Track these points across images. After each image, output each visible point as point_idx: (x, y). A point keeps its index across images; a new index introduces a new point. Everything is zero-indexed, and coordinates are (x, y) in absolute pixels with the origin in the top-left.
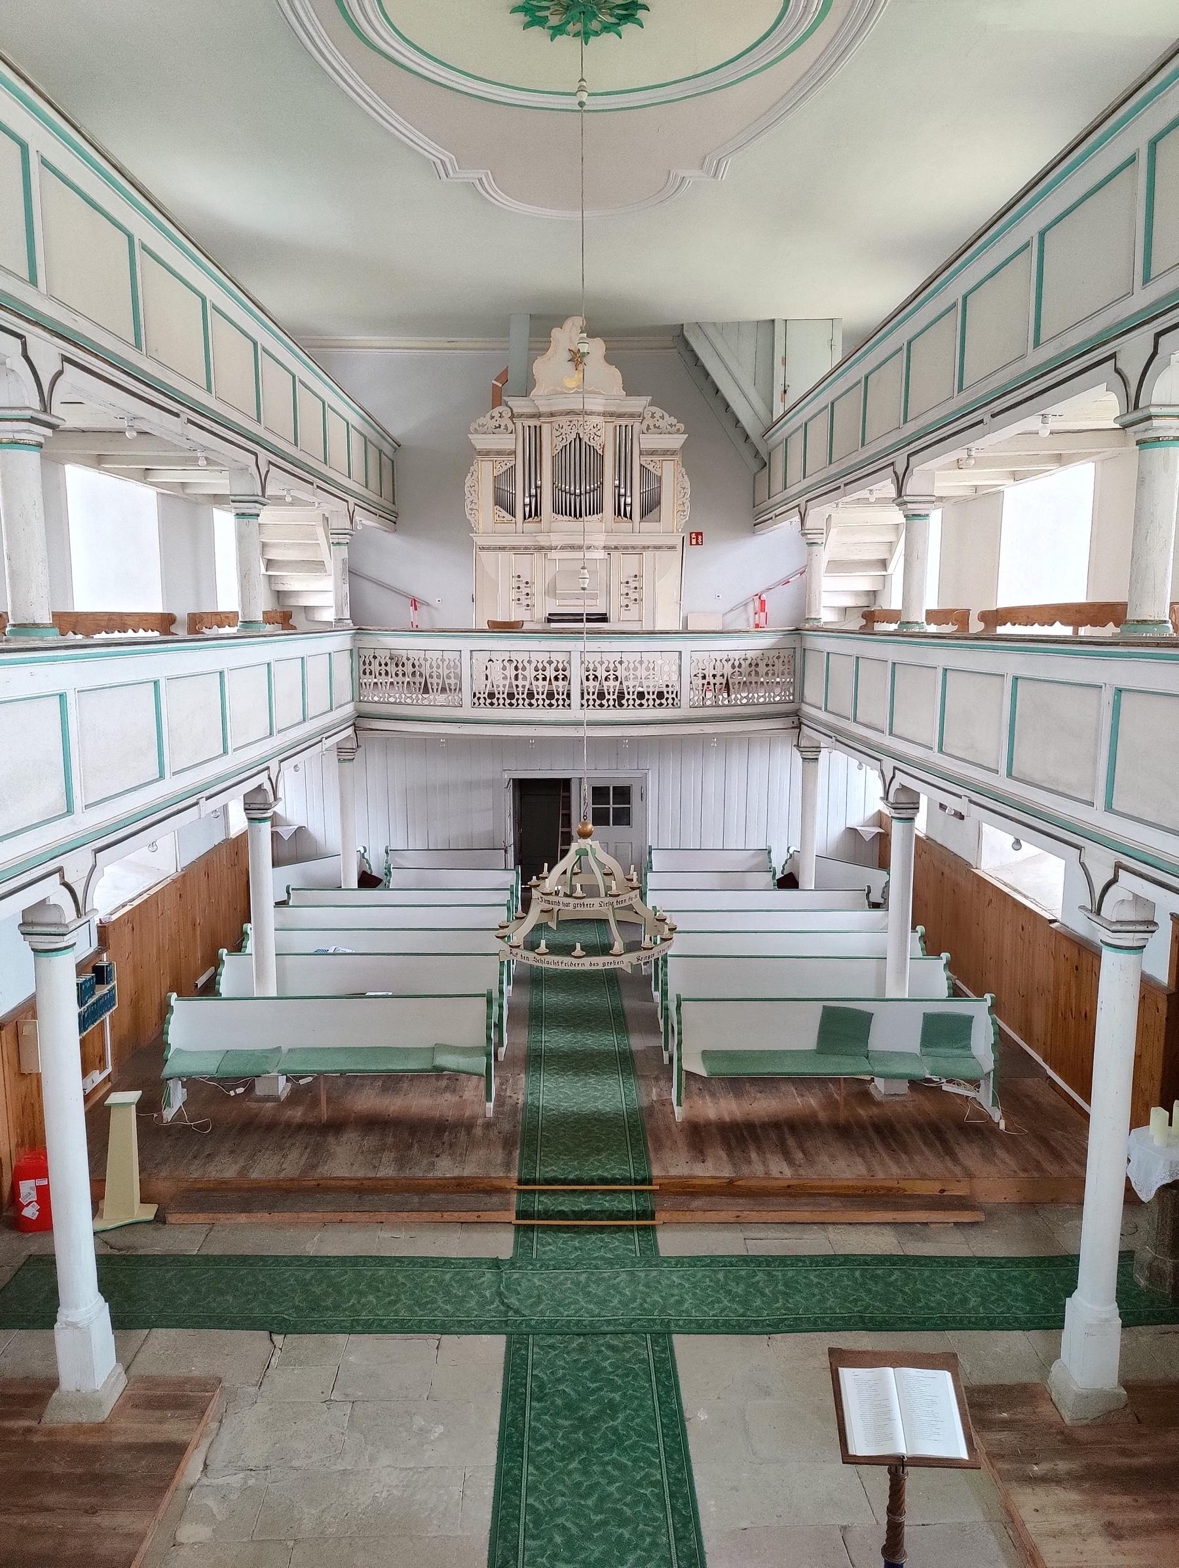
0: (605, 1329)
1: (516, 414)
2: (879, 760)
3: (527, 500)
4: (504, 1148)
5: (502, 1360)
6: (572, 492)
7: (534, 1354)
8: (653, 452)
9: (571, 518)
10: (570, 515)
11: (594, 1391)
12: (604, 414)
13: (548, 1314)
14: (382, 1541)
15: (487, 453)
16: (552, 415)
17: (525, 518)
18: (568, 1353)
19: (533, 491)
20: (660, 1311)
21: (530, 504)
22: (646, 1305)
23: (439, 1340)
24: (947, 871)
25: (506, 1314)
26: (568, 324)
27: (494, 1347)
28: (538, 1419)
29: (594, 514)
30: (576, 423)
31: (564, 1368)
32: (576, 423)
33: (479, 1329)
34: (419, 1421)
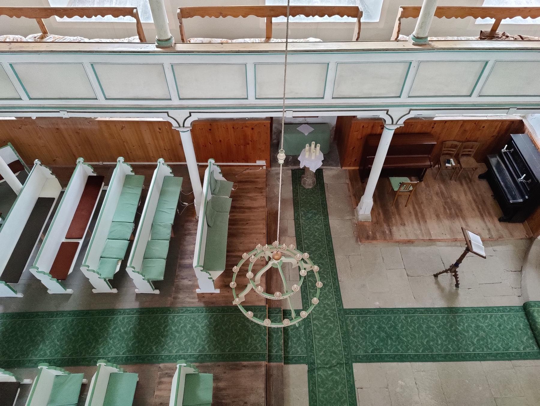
0: (345, 329)
2: (167, 113)
4: (239, 369)
5: (362, 363)
7: (361, 353)
11: (375, 333)
13: (341, 349)
14: (446, 393)
18: (359, 341)
20: (334, 311)
22: (332, 315)
23: (357, 389)
24: (62, 127)
25: (341, 364)
27: (358, 369)
28: (390, 350)
31: (366, 343)
33: (350, 374)
34: (398, 390)
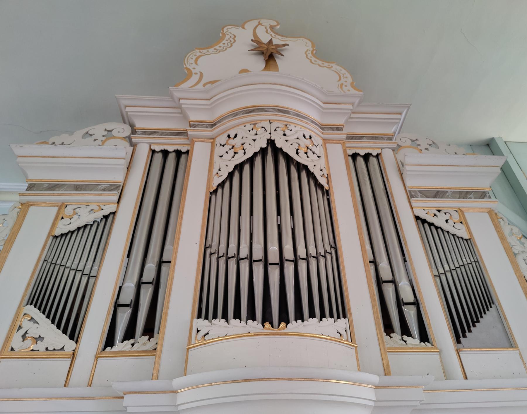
1: (140, 131)
3: (127, 297)
6: (258, 254)
8: (438, 194)
9: (255, 326)
10: (252, 316)
12: (323, 127)
15: (53, 187)
16: (213, 125)
17: (110, 342)
19: (151, 266)
21: (135, 306)
26: (250, 26)
29: (323, 315)
30: (266, 125)
32: (266, 125)
